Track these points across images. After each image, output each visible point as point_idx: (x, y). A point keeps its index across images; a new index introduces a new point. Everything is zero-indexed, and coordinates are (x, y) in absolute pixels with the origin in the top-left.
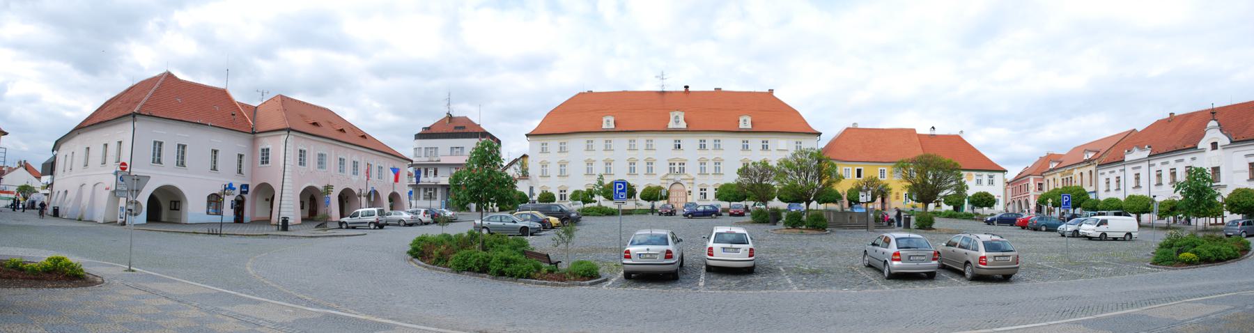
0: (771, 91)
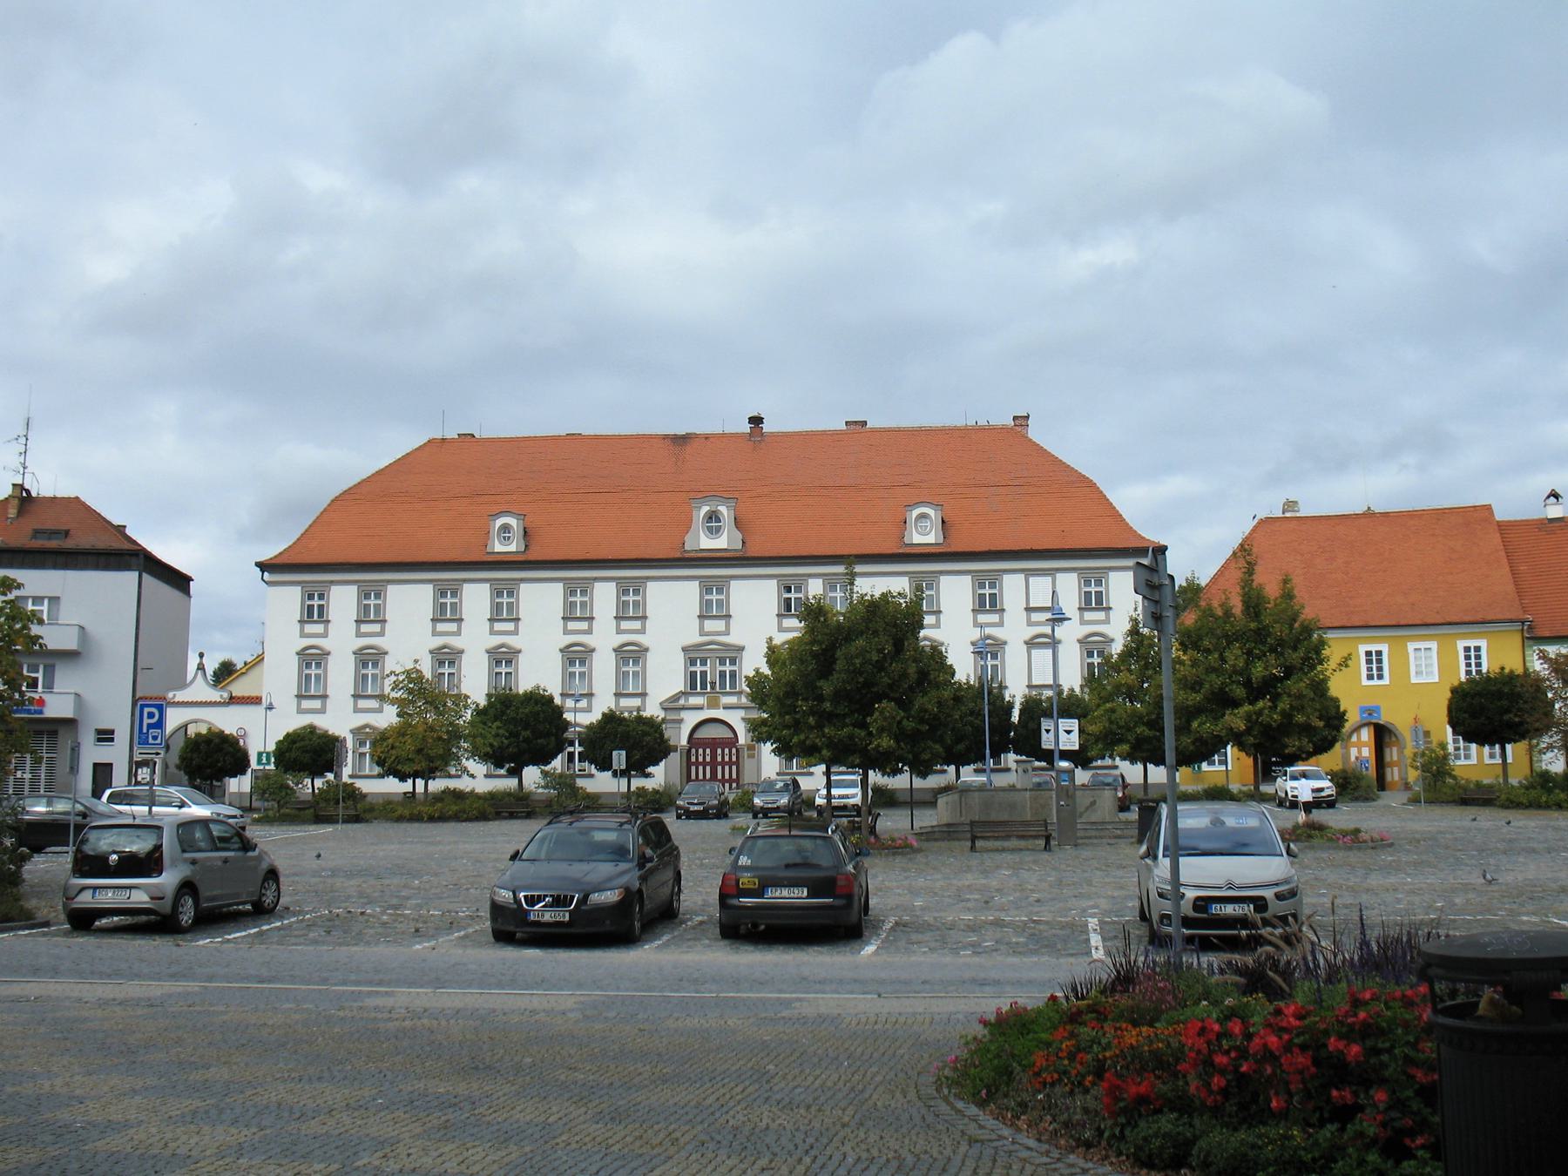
0: (1022, 420)
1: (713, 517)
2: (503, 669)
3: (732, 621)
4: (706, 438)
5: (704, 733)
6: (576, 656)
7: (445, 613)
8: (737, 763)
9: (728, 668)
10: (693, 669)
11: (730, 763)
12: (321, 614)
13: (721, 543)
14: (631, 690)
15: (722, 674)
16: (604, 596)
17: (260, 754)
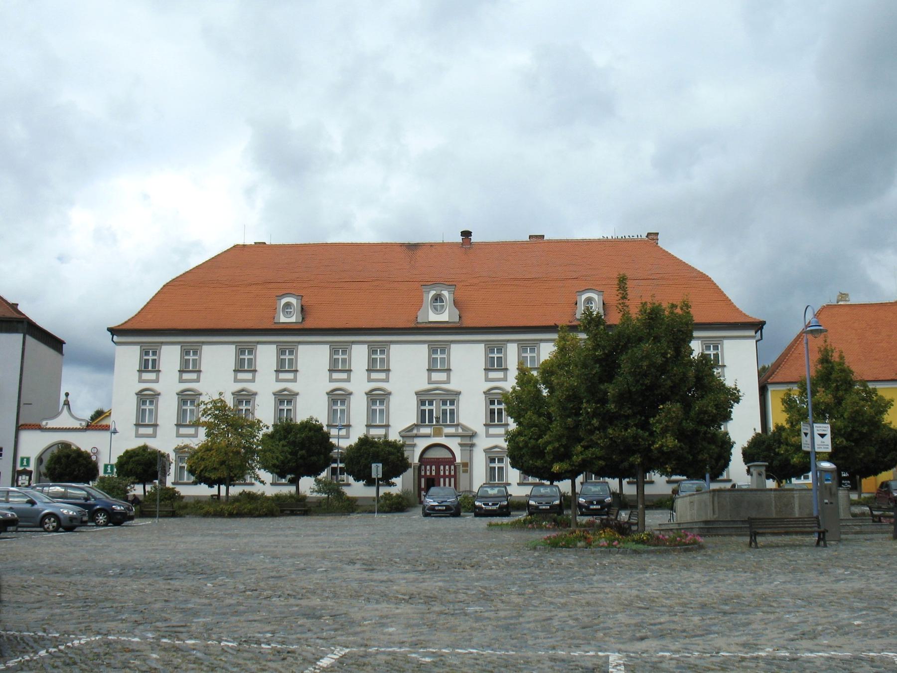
1: (438, 298)
2: (285, 407)
3: (452, 374)
4: (431, 246)
5: (432, 454)
6: (338, 398)
7: (245, 366)
8: (455, 476)
9: (448, 407)
10: (423, 408)
11: (450, 477)
12: (154, 366)
13: (444, 317)
14: (378, 423)
15: (444, 412)
16: (359, 355)
17: (106, 466)
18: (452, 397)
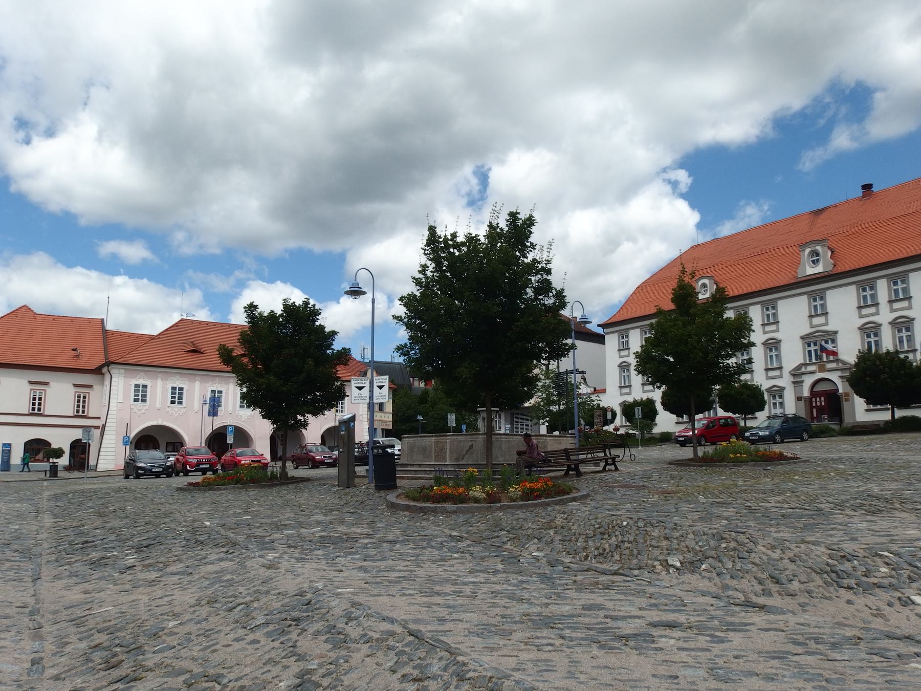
3: (829, 316)
5: (819, 388)
13: (819, 269)
18: (832, 336)
